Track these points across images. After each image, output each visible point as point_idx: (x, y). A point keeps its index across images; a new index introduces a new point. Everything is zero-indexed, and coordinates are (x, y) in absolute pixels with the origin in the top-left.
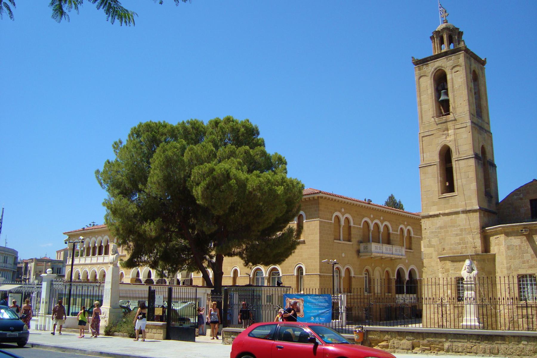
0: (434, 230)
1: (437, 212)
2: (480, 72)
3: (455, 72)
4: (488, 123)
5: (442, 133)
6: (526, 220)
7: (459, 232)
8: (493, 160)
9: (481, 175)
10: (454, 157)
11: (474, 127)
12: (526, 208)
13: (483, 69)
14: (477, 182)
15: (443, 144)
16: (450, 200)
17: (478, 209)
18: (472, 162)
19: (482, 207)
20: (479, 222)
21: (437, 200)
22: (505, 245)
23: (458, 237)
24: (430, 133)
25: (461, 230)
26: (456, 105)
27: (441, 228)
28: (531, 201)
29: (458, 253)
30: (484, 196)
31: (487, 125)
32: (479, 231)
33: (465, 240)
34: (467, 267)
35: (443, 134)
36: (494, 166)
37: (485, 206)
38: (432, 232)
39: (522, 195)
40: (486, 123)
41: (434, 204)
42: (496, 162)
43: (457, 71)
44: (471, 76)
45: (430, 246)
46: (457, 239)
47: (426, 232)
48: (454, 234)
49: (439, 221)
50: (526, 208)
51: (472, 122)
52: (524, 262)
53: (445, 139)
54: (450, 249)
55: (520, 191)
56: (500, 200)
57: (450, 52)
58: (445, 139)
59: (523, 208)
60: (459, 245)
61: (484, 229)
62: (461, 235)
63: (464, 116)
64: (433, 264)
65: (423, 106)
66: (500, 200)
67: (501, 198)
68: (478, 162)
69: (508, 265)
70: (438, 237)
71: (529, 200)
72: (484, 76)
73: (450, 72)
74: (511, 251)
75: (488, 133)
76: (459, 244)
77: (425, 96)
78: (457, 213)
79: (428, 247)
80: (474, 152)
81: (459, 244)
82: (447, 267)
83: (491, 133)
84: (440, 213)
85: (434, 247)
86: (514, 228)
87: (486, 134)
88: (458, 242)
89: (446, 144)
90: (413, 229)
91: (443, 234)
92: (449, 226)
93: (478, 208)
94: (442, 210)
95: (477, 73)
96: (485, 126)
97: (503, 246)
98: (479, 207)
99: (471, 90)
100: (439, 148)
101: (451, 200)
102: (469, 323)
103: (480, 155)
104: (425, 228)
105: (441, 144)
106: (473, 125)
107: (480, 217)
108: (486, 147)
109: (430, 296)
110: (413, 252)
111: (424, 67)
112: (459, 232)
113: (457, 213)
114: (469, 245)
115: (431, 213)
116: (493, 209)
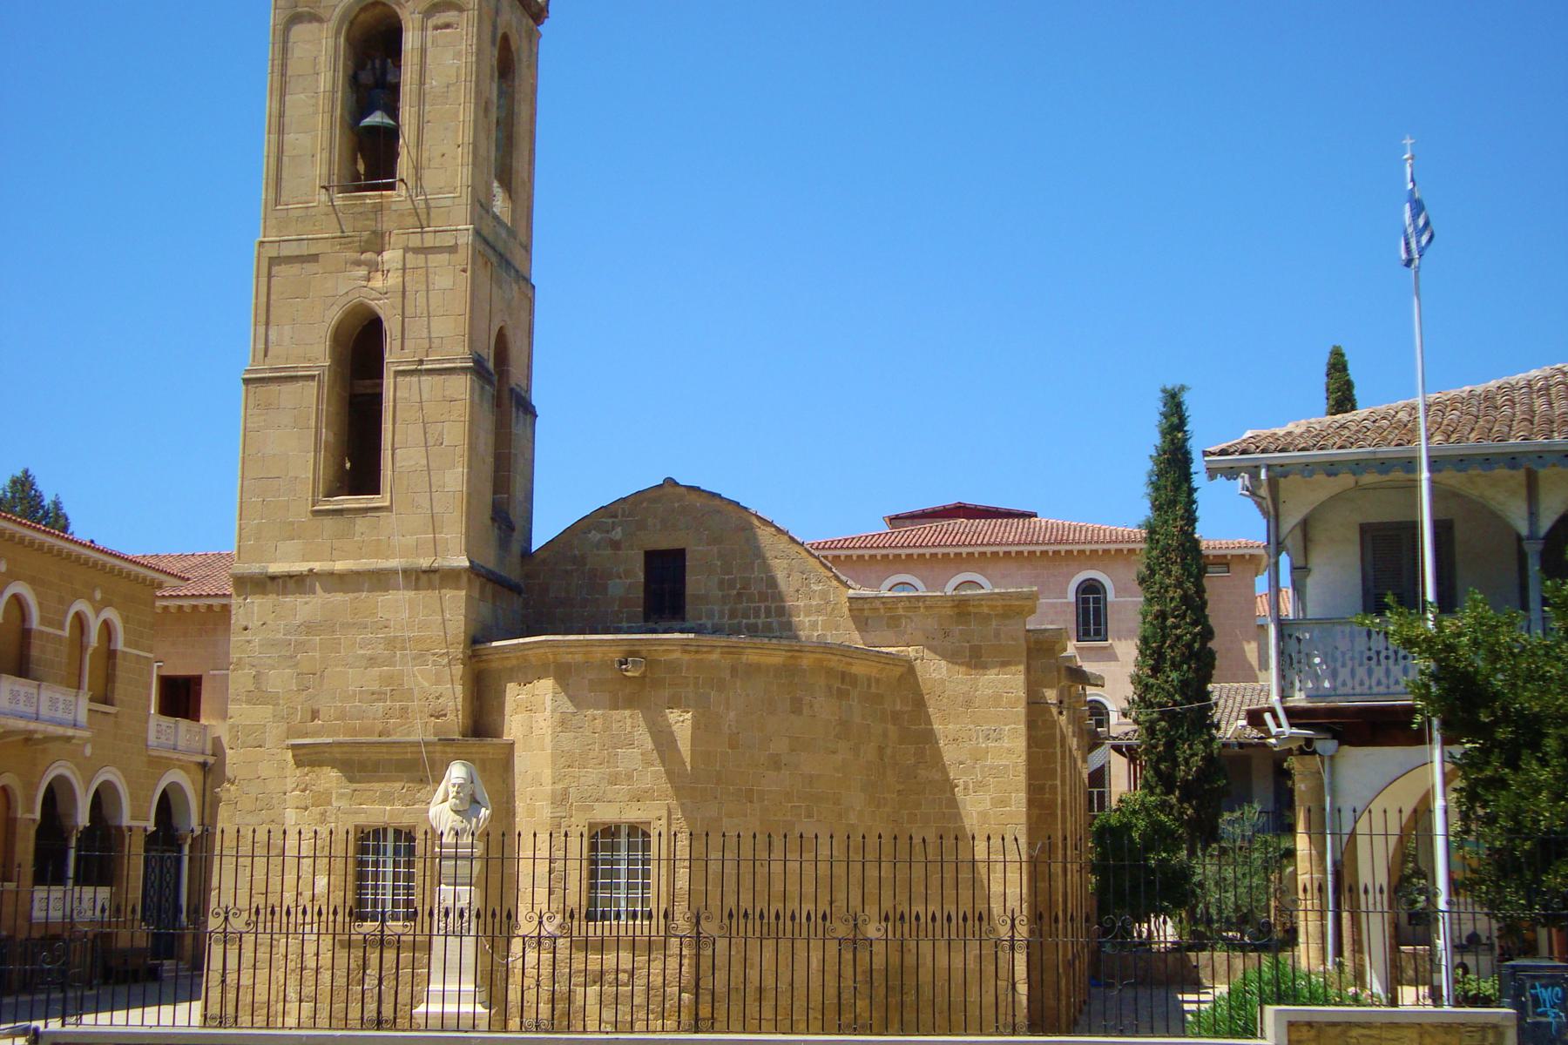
0: (280, 636)
1: (301, 567)
2: (525, 45)
3: (436, 28)
4: (527, 248)
5: (356, 256)
6: (625, 625)
7: (380, 650)
8: (529, 390)
9: (486, 441)
10: (393, 357)
11: (483, 255)
12: (629, 581)
13: (533, 38)
14: (470, 467)
15: (355, 298)
17: (466, 570)
18: (461, 387)
19: (477, 561)
20: (462, 617)
21: (305, 517)
22: (553, 711)
24: (304, 249)
25: (391, 643)
26: (425, 155)
27: (309, 627)
28: (652, 557)
29: (370, 732)
30: (489, 522)
31: (523, 252)
32: (458, 651)
34: (452, 791)
35: (358, 263)
36: (529, 411)
37: (490, 561)
38: (273, 644)
39: (619, 529)
40: (521, 244)
42: (537, 399)
43: (447, 26)
44: (492, 55)
45: (258, 696)
46: (372, 679)
47: (248, 642)
48: (363, 655)
49: (306, 603)
50: (629, 581)
51: (477, 232)
52: (614, 780)
53: (364, 283)
54: (342, 716)
55: (616, 517)
56: (537, 543)
58: (364, 283)
59: (618, 581)
60: (379, 700)
61: (478, 647)
62: (390, 662)
63: (449, 202)
64: (265, 769)
65: (289, 138)
66: (537, 543)
67: (541, 536)
68: (482, 388)
69: (559, 787)
70: (296, 665)
71: (642, 553)
72: (534, 65)
73: (418, 24)
74: (572, 735)
75: (522, 283)
76: (379, 696)
77: (302, 96)
78: (379, 580)
79: (249, 702)
80: (470, 347)
81: (379, 696)
83: (534, 287)
84: (311, 570)
86: (595, 649)
87: (515, 287)
88: (376, 688)
90: (126, 620)
93: (467, 564)
95: (514, 48)
96: (517, 258)
97: (548, 713)
98: (471, 562)
99: (486, 110)
100: (334, 315)
101: (361, 523)
102: (451, 1008)
103: (491, 365)
104: (245, 623)
106: (481, 247)
107: (469, 598)
108: (509, 333)
109: (746, 904)
110: (116, 715)
112: (380, 650)
113: (379, 580)
115: (275, 568)
116: (513, 572)
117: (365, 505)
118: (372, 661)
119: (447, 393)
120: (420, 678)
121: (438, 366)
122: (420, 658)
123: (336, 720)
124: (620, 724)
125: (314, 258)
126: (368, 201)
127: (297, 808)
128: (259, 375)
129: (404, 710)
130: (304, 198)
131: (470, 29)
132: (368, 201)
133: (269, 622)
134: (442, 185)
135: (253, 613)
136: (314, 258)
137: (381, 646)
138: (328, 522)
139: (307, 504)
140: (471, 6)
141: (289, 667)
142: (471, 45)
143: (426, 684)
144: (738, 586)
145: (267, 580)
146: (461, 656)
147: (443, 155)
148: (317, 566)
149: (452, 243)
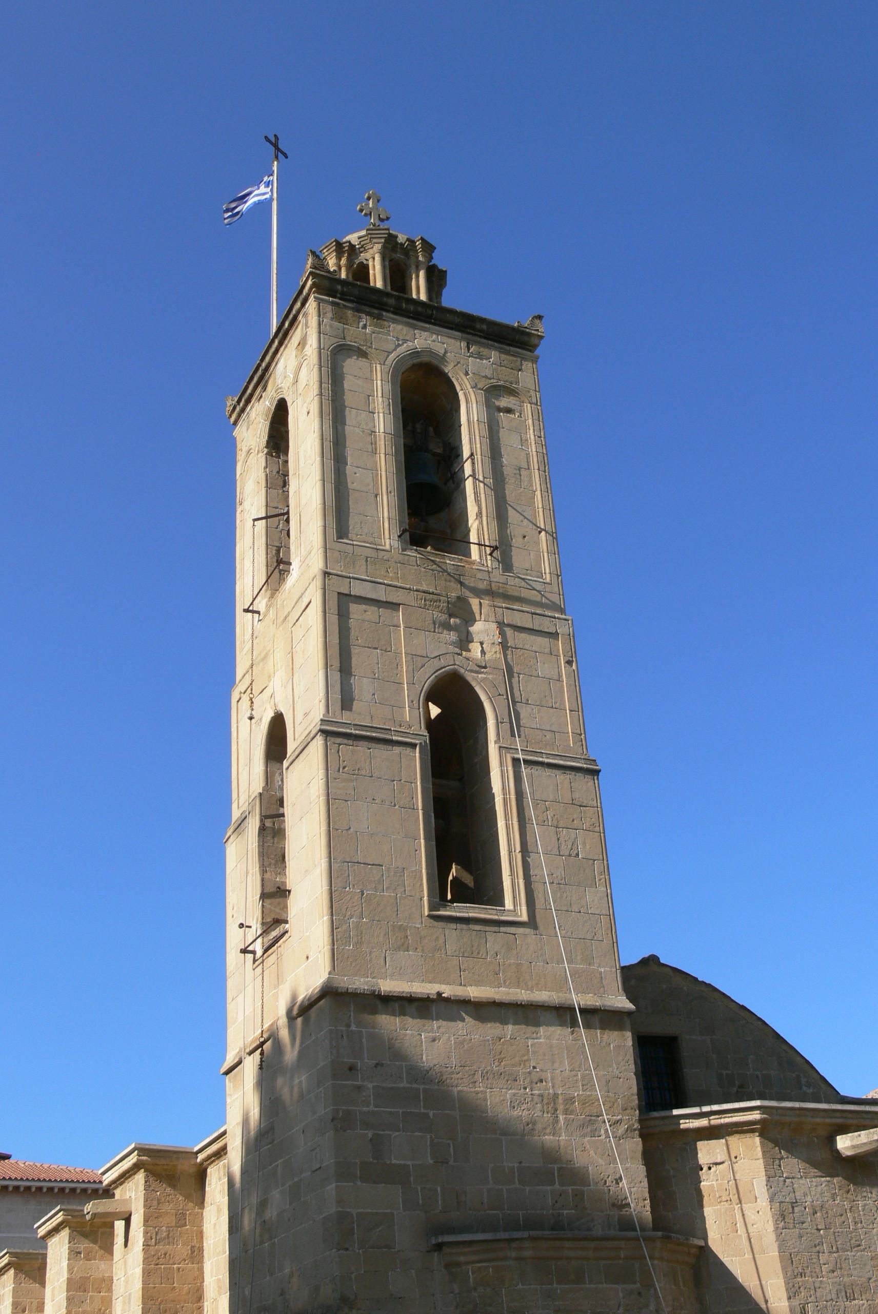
0: (404, 1084)
16: (491, 937)
24: (381, 594)
47: (359, 1088)
57: (484, 327)
89: (462, 671)
94: (448, 984)
105: (436, 664)
111: (365, 319)
115: (388, 986)
117: (496, 917)
119: (576, 795)
120: (592, 1152)
121: (561, 762)
124: (843, 1218)
125: (394, 606)
126: (448, 562)
128: (335, 729)
130: (371, 539)
131: (536, 422)
132: (448, 562)
134: (527, 566)
136: (394, 606)
138: (452, 932)
139: (422, 906)
140: (534, 400)
142: (540, 437)
144: (737, 1083)
145: (378, 1002)
146: (637, 1126)
147: (524, 537)
148: (448, 991)
149: (552, 630)
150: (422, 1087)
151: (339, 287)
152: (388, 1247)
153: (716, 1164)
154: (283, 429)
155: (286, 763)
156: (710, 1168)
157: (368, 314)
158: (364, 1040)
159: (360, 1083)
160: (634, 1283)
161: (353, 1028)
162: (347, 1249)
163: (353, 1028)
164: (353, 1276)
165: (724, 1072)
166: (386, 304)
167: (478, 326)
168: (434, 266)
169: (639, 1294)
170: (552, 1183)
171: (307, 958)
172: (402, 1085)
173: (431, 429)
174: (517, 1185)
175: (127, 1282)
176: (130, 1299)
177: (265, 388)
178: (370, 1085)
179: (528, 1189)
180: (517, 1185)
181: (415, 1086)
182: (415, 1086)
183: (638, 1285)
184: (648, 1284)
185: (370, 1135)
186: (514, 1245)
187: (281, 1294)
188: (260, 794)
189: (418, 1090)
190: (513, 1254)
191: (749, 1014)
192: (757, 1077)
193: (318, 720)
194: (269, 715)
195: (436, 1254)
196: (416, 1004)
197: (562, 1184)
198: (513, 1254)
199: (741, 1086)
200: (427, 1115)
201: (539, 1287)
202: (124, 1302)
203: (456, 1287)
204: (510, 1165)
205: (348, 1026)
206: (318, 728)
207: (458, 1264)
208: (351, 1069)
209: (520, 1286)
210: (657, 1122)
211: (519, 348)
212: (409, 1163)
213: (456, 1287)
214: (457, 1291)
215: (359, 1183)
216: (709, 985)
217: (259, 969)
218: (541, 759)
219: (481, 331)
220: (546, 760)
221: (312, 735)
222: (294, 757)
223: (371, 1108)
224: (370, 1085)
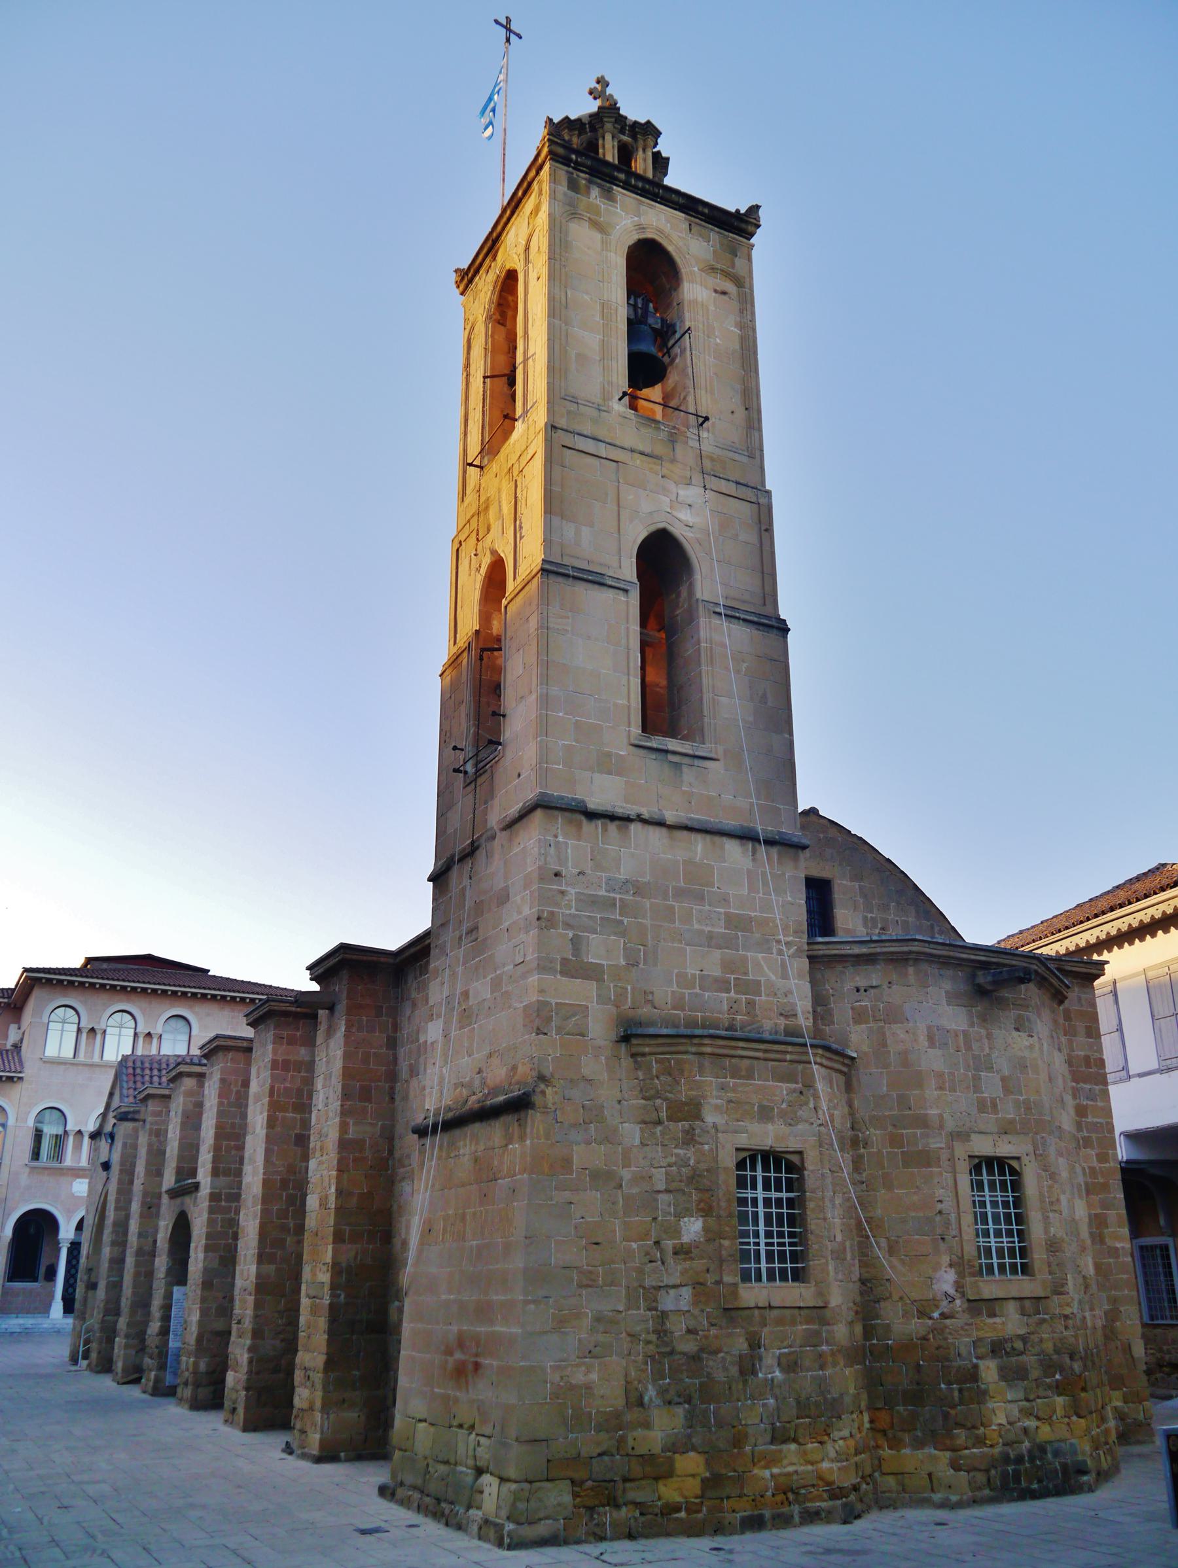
0: (602, 893)
16: (685, 769)
23: (717, 954)
25: (731, 921)
33: (746, 974)
41: (607, 764)
46: (712, 963)
47: (563, 893)
48: (701, 932)
52: (982, 1107)
70: (623, 934)
76: (722, 985)
79: (562, 973)
81: (722, 985)
82: (684, 1092)
85: (599, 980)
88: (717, 972)
91: (648, 922)
92: (680, 893)
114: (763, 998)
118: (711, 940)
122: (764, 945)
123: (674, 1008)
127: (645, 1122)
129: (750, 1004)
133: (589, 872)
135: (567, 858)
137: (722, 923)
141: (615, 934)
143: (773, 977)
144: (880, 926)
150: (618, 896)
151: (574, 157)
152: (583, 1035)
153: (872, 987)
154: (510, 298)
155: (504, 602)
156: (865, 991)
157: (599, 186)
158: (569, 851)
159: (563, 888)
160: (797, 1083)
161: (560, 839)
162: (546, 1034)
163: (560, 839)
164: (550, 1058)
165: (869, 915)
166: (616, 179)
167: (700, 208)
168: (659, 153)
169: (801, 1093)
170: (728, 992)
171: (519, 775)
172: (600, 893)
173: (651, 305)
174: (697, 990)
175: (328, 1062)
176: (331, 1077)
177: (494, 259)
178: (573, 891)
179: (707, 994)
180: (697, 990)
181: (612, 895)
182: (612, 895)
183: (800, 1085)
184: (809, 1085)
185: (571, 935)
186: (696, 1041)
187: (479, 1073)
188: (477, 632)
189: (615, 899)
190: (693, 1049)
191: (892, 866)
192: (897, 921)
193: (539, 561)
194: (487, 561)
195: (623, 1045)
196: (617, 823)
197: (736, 993)
198: (693, 1049)
199: (883, 929)
200: (621, 922)
201: (714, 1080)
202: (325, 1079)
203: (640, 1075)
204: (693, 972)
205: (556, 836)
206: (539, 567)
207: (644, 1055)
208: (556, 875)
209: (698, 1077)
210: (820, 947)
211: (737, 234)
212: (604, 963)
213: (640, 1075)
214: (641, 1078)
215: (559, 977)
216: (861, 838)
217: (469, 789)
218: (737, 615)
219: (703, 214)
220: (742, 616)
221: (533, 573)
222: (512, 595)
223: (573, 911)
224: (573, 891)
